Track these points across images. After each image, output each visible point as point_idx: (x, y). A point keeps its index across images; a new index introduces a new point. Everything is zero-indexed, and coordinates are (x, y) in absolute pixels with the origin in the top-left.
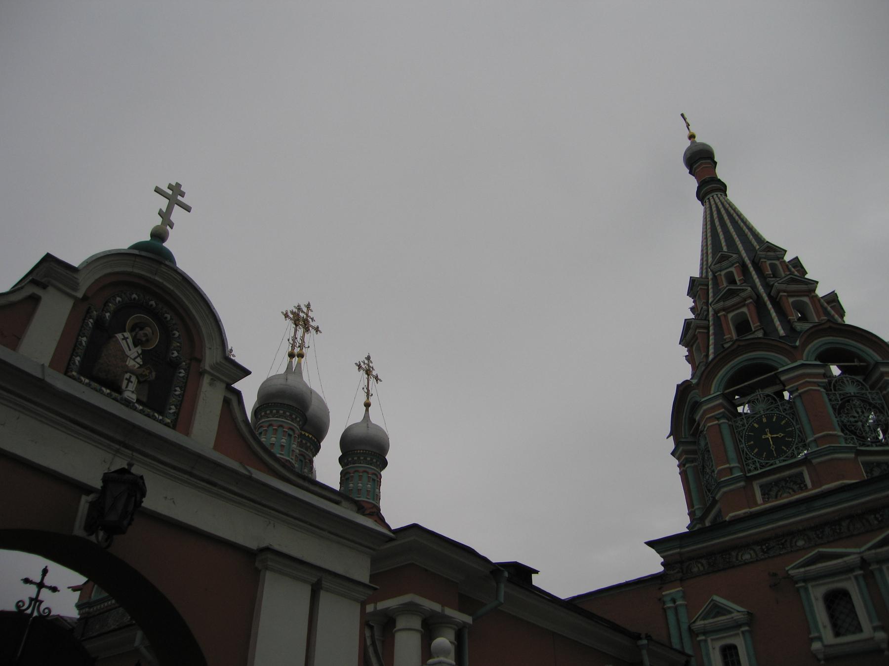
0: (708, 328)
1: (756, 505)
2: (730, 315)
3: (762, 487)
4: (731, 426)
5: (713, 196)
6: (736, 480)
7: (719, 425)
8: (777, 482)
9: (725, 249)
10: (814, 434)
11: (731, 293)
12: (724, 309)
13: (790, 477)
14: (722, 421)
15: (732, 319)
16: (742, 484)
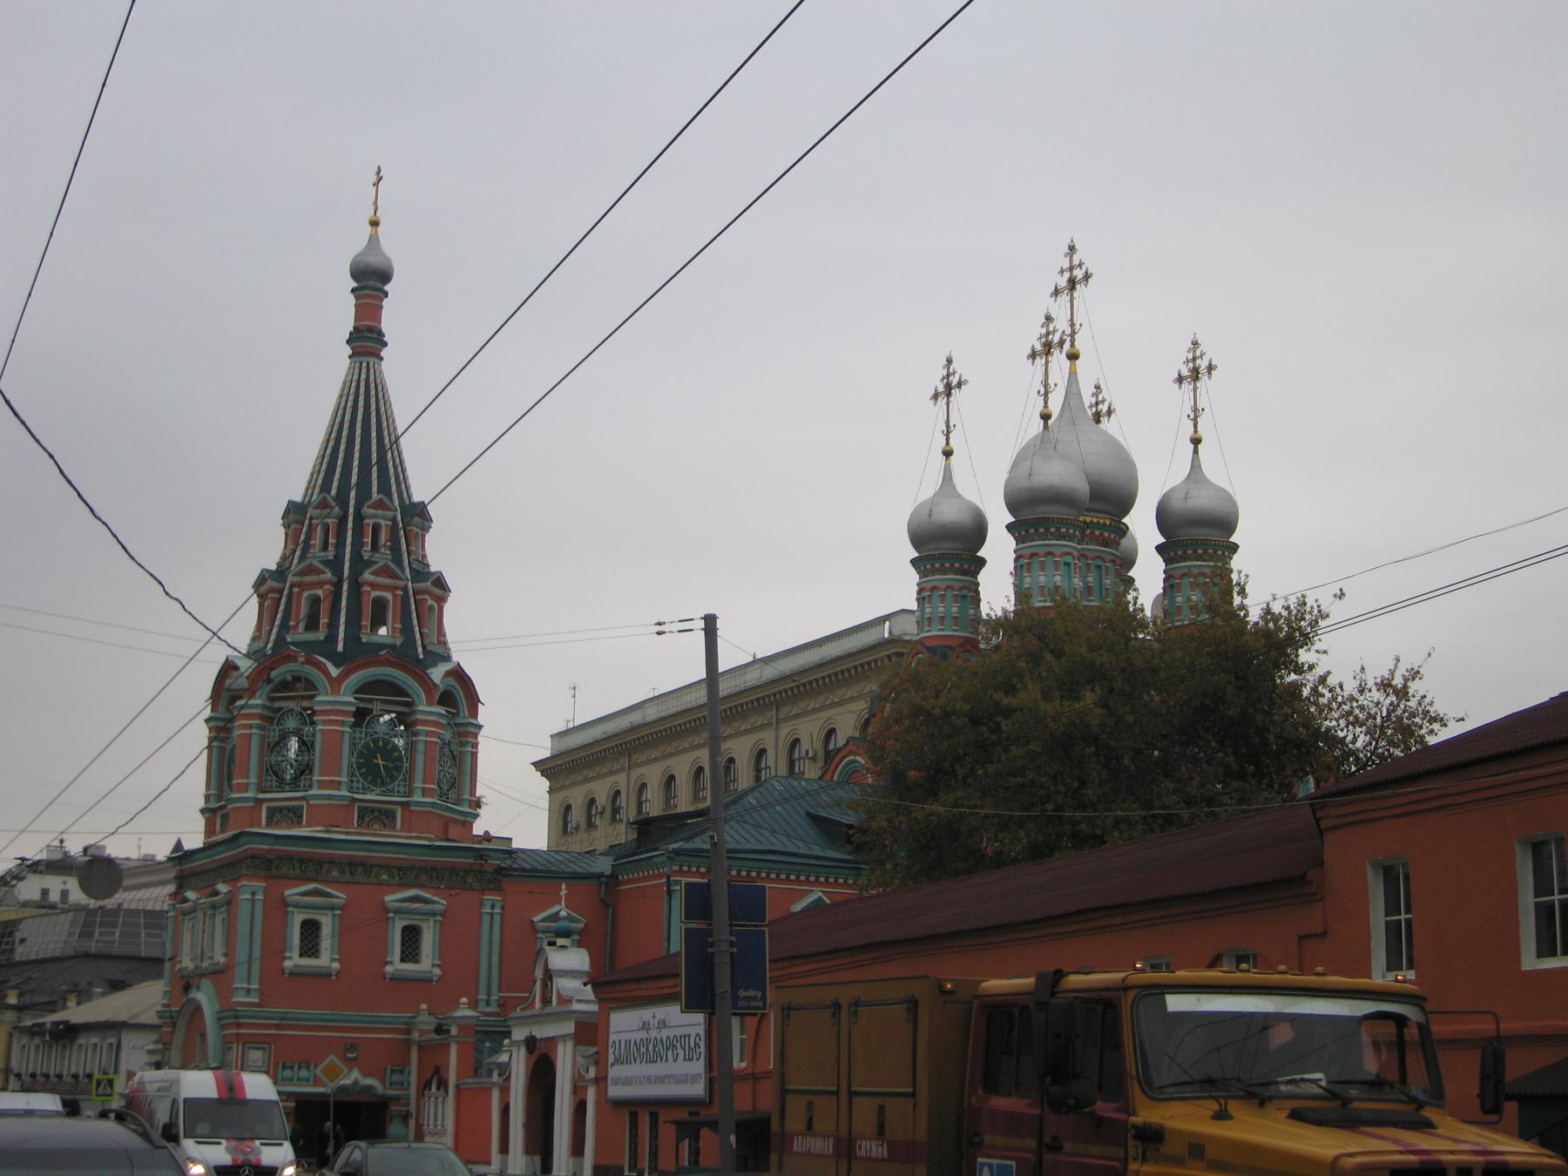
0: (281, 592)
1: (259, 825)
2: (306, 594)
3: (269, 809)
4: (263, 737)
5: (361, 364)
6: (247, 799)
7: (251, 734)
8: (281, 810)
9: (333, 492)
10: (321, 776)
11: (310, 570)
12: (300, 585)
13: (293, 807)
14: (254, 731)
15: (309, 597)
16: (251, 804)
